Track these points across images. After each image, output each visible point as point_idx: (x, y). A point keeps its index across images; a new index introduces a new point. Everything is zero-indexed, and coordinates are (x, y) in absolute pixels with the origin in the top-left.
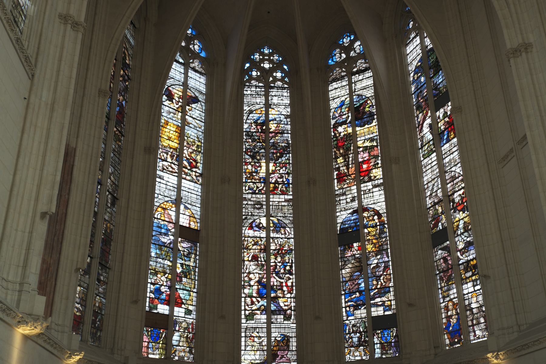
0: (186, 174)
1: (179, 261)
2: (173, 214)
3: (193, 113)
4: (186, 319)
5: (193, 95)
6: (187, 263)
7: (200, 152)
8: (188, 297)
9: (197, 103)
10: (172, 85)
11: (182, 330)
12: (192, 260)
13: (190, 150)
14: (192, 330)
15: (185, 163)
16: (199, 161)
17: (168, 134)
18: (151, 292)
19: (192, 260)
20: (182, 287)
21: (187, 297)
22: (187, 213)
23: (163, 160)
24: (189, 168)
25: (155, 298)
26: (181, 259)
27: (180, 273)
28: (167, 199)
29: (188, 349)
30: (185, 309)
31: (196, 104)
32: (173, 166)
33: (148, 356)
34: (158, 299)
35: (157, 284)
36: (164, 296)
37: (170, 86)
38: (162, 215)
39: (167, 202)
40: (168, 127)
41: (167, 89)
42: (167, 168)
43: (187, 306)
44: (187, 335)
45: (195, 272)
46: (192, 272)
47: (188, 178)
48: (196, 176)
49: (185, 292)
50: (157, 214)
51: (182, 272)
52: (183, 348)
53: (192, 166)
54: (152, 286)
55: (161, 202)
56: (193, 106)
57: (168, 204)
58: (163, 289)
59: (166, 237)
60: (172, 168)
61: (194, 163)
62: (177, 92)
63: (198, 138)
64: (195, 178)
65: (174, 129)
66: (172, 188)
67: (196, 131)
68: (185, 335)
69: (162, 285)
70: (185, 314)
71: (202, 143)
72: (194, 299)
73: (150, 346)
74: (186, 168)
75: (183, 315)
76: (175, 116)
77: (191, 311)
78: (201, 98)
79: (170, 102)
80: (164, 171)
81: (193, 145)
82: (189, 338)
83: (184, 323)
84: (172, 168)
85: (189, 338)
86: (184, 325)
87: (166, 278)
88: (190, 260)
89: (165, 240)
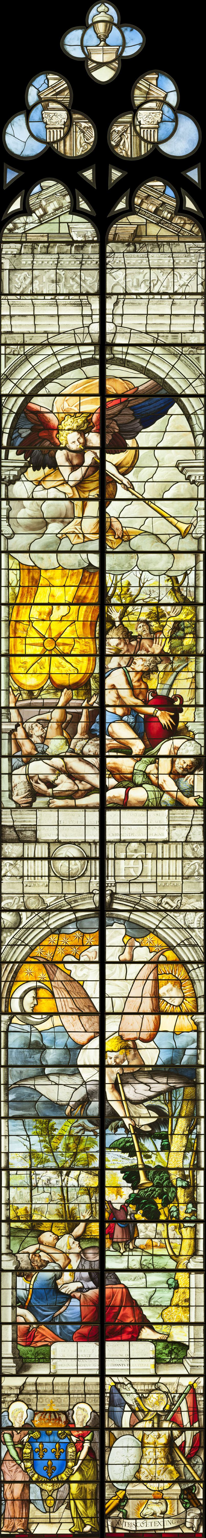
0: (127, 781)
1: (116, 1159)
2: (88, 974)
3: (145, 474)
4: (163, 1380)
5: (141, 382)
6: (154, 1162)
7: (187, 654)
8: (169, 1294)
9: (162, 412)
10: (43, 383)
11: (148, 1425)
12: (177, 1143)
13: (140, 664)
14: (194, 1418)
15: (121, 731)
16: (187, 696)
17: (42, 627)
18: (19, 1302)
19: (177, 1143)
20: (135, 1263)
21: (164, 1296)
22: (142, 954)
23: (29, 758)
24: (138, 746)
25: (38, 1323)
26: (124, 1150)
27: (124, 1207)
28: (56, 920)
29: (177, 1488)
30: (154, 1341)
31: (159, 424)
32: (75, 764)
33: (27, 1529)
34: (51, 1323)
35: (41, 1269)
36: (73, 1310)
37: (34, 393)
38: (42, 993)
39: (58, 930)
40: (42, 595)
41: (25, 412)
42: (51, 785)
43: (165, 1329)
44: (171, 1440)
45: (191, 1187)
46: (181, 1193)
47: (137, 794)
48: (175, 775)
49: (153, 1278)
50: (18, 994)
51: (135, 1200)
52: (154, 1486)
53: (152, 734)
54: (21, 1282)
55: (33, 937)
56: (145, 438)
57: (63, 940)
58: (68, 1284)
59: (64, 1079)
60: (72, 776)
61: (164, 718)
62: (71, 404)
63: (176, 589)
64: (169, 784)
65: (69, 595)
66: (76, 866)
67: (163, 562)
68: (163, 1440)
69: (63, 1270)
70: (158, 1361)
71: (195, 604)
72: (197, 1297)
73: (35, 1492)
74: (127, 752)
75: (148, 1366)
76: (70, 528)
77: (184, 1347)
78: (181, 375)
79: (40, 474)
80: (40, 802)
81: (153, 636)
82: (182, 1448)
83: (154, 1397)
84: (72, 776)
85: (182, 1448)
86: (156, 1402)
87: (78, 1239)
88: (166, 1148)
89: (60, 1090)
